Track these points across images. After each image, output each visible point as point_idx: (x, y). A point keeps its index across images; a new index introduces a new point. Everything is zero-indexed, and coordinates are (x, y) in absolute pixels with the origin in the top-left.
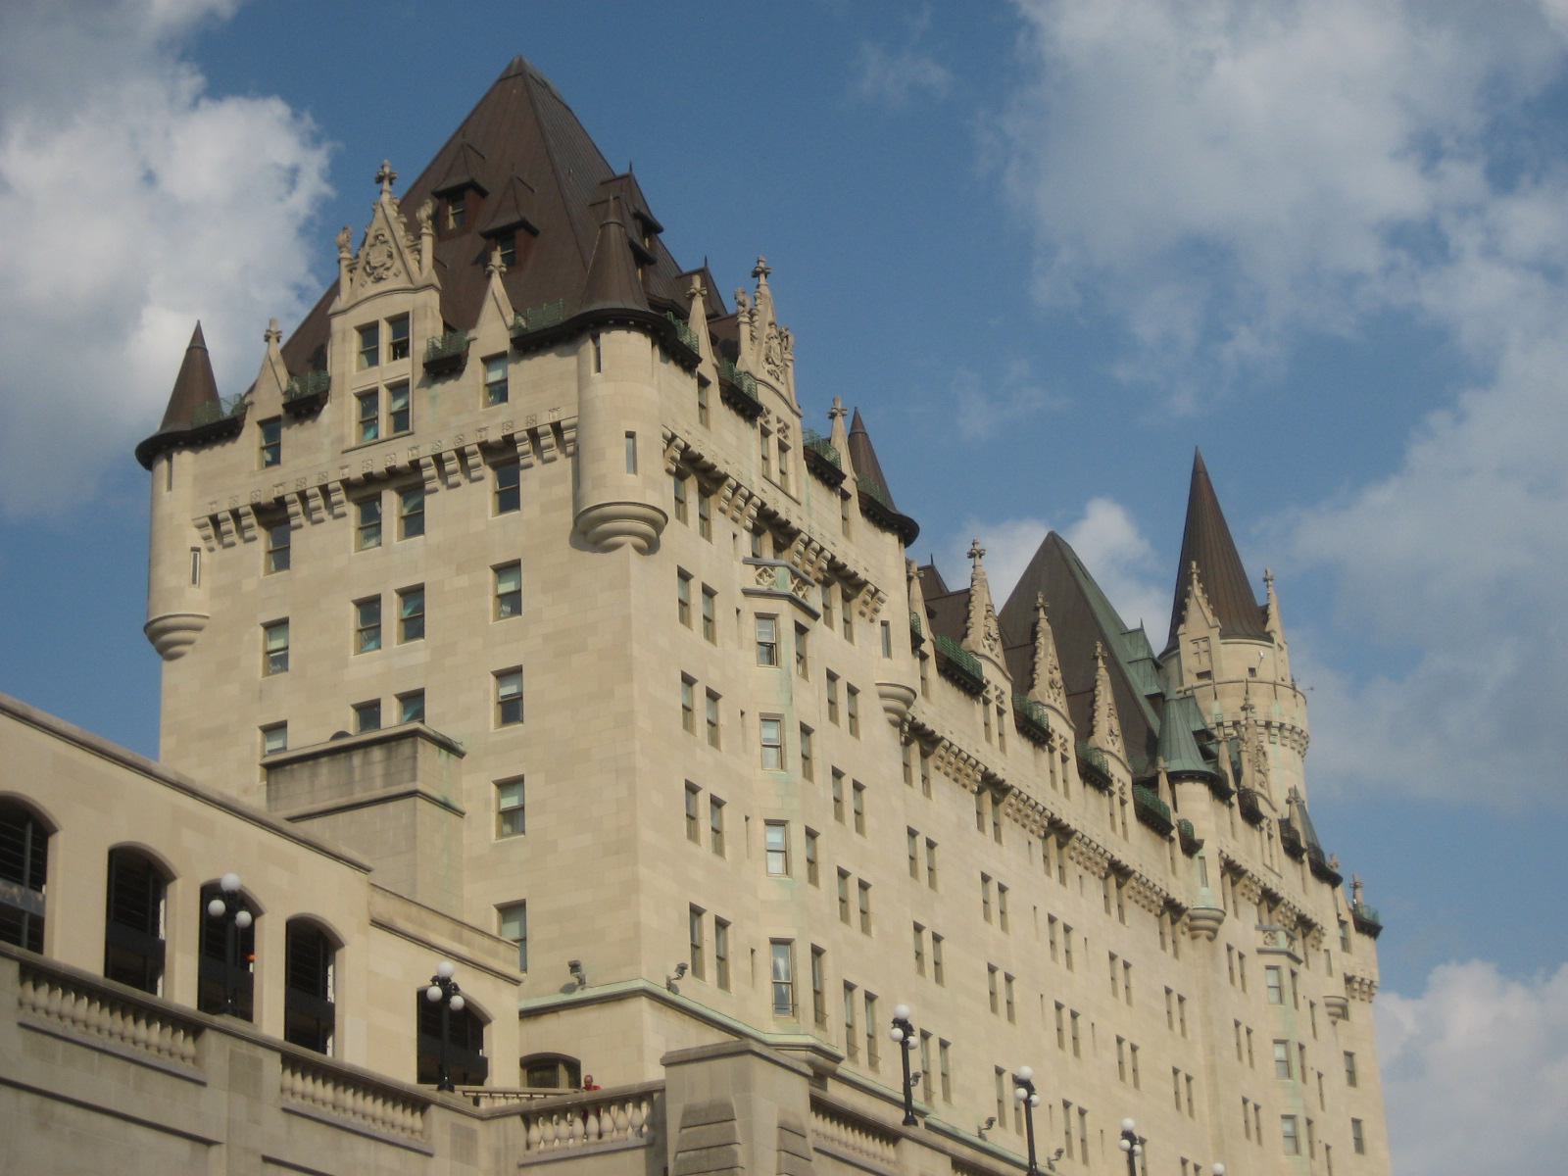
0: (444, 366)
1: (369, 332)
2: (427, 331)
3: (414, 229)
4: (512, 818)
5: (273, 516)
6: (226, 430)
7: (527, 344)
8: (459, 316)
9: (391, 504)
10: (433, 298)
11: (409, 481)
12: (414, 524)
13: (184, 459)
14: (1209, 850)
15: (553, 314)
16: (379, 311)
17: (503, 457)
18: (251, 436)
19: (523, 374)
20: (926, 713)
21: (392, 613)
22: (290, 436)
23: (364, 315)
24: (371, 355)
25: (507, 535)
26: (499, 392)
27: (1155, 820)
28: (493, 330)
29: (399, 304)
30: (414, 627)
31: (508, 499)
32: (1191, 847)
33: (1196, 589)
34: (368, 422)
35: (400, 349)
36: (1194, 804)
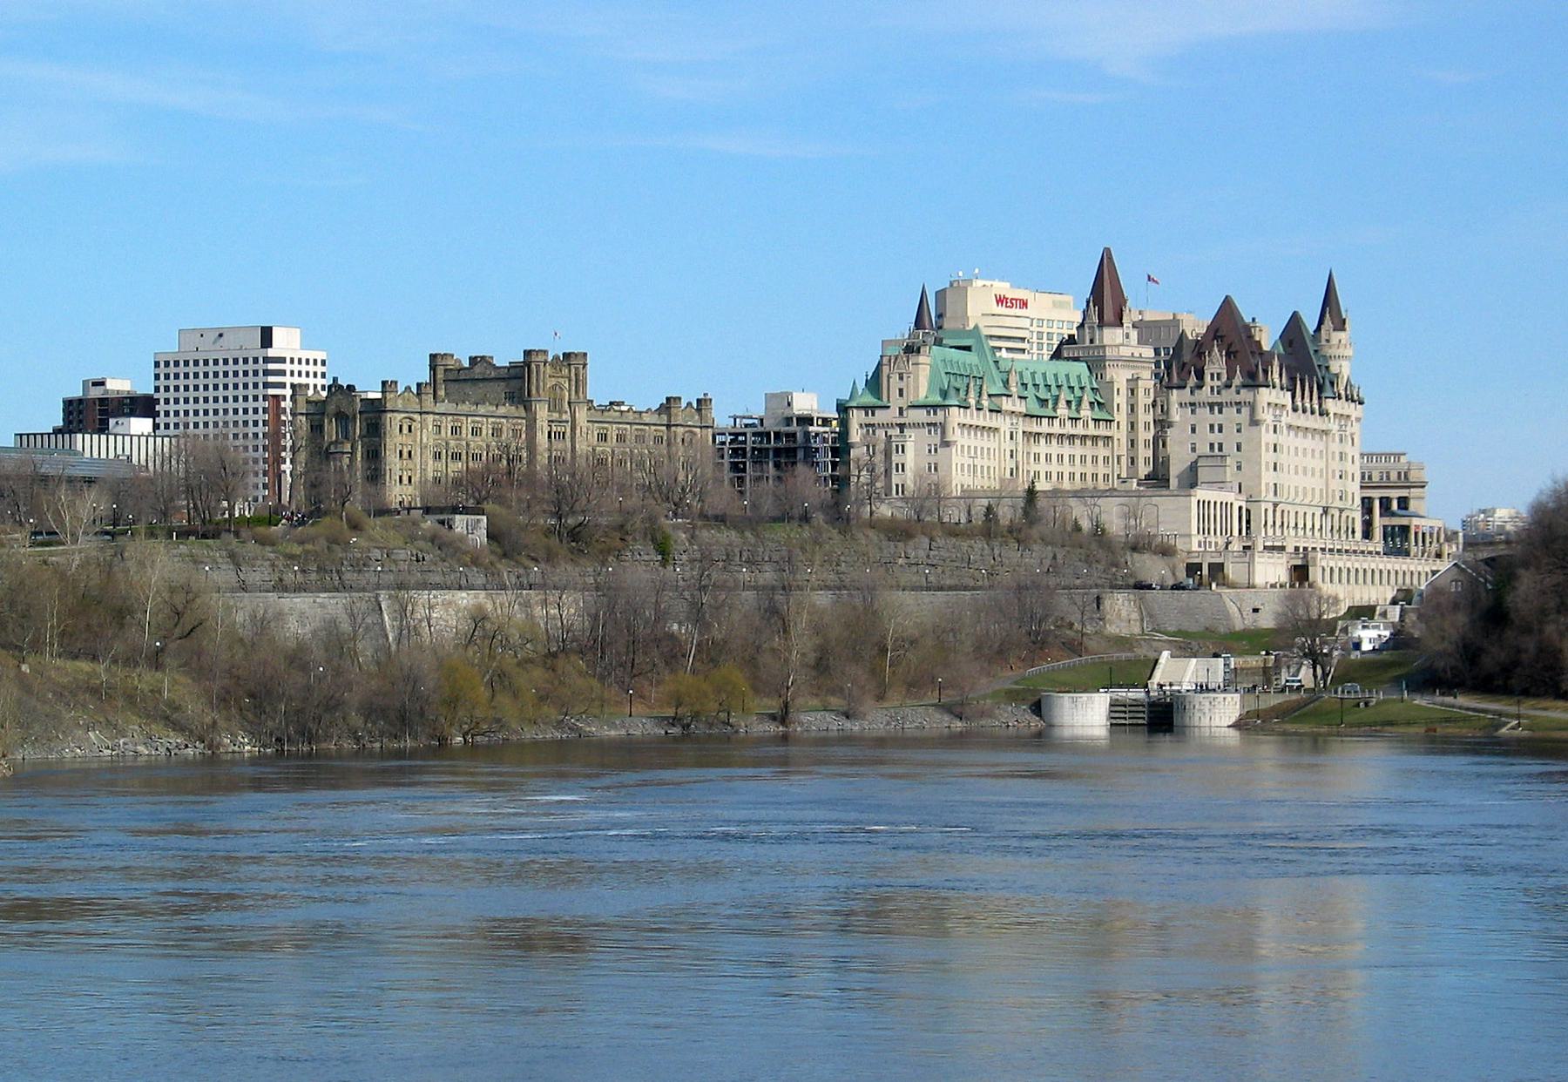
1: (1212, 375)
3: (1221, 355)
4: (1239, 468)
5: (1192, 404)
7: (1244, 386)
8: (1231, 376)
9: (1216, 408)
10: (1225, 371)
11: (1220, 405)
12: (1220, 412)
13: (1175, 391)
14: (1331, 415)
15: (1250, 382)
16: (1215, 371)
17: (1238, 404)
18: (1188, 389)
19: (1243, 391)
21: (1216, 428)
22: (1197, 392)
24: (1212, 379)
26: (1238, 393)
28: (1238, 380)
29: (1219, 371)
30: (1220, 430)
31: (1239, 411)
33: (1328, 315)
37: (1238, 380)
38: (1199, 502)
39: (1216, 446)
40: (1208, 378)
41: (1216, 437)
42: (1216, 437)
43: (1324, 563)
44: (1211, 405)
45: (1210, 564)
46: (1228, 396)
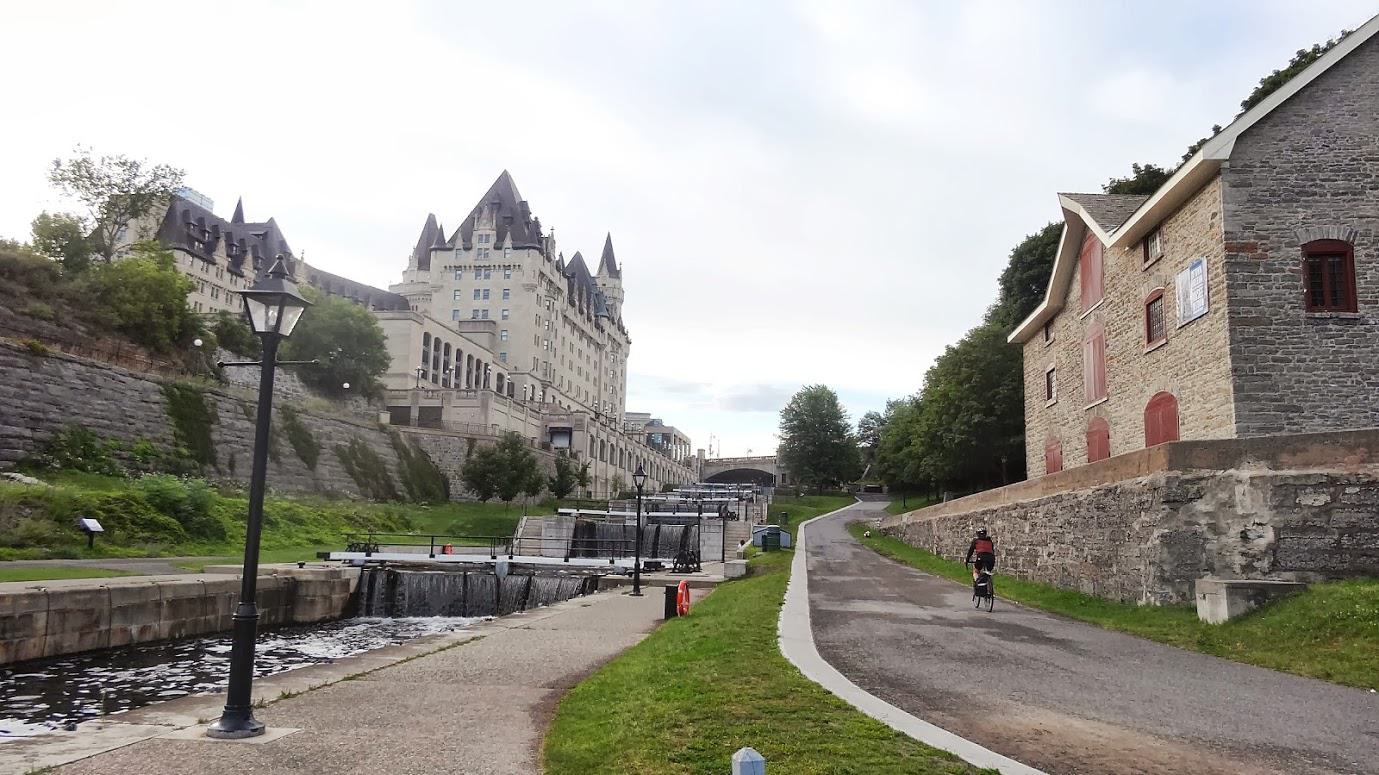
0: (497, 248)
2: (493, 240)
6: (450, 249)
8: (501, 238)
11: (488, 268)
12: (487, 277)
20: (567, 314)
21: (481, 294)
23: (480, 232)
25: (507, 284)
27: (598, 326)
28: (508, 243)
29: (488, 232)
30: (486, 297)
32: (603, 331)
34: (479, 254)
35: (487, 241)
36: (605, 322)
37: (508, 243)
38: (427, 336)
39: (480, 314)
40: (474, 240)
41: (480, 304)
42: (480, 304)
43: (593, 431)
44: (478, 268)
45: (422, 409)
46: (496, 258)
